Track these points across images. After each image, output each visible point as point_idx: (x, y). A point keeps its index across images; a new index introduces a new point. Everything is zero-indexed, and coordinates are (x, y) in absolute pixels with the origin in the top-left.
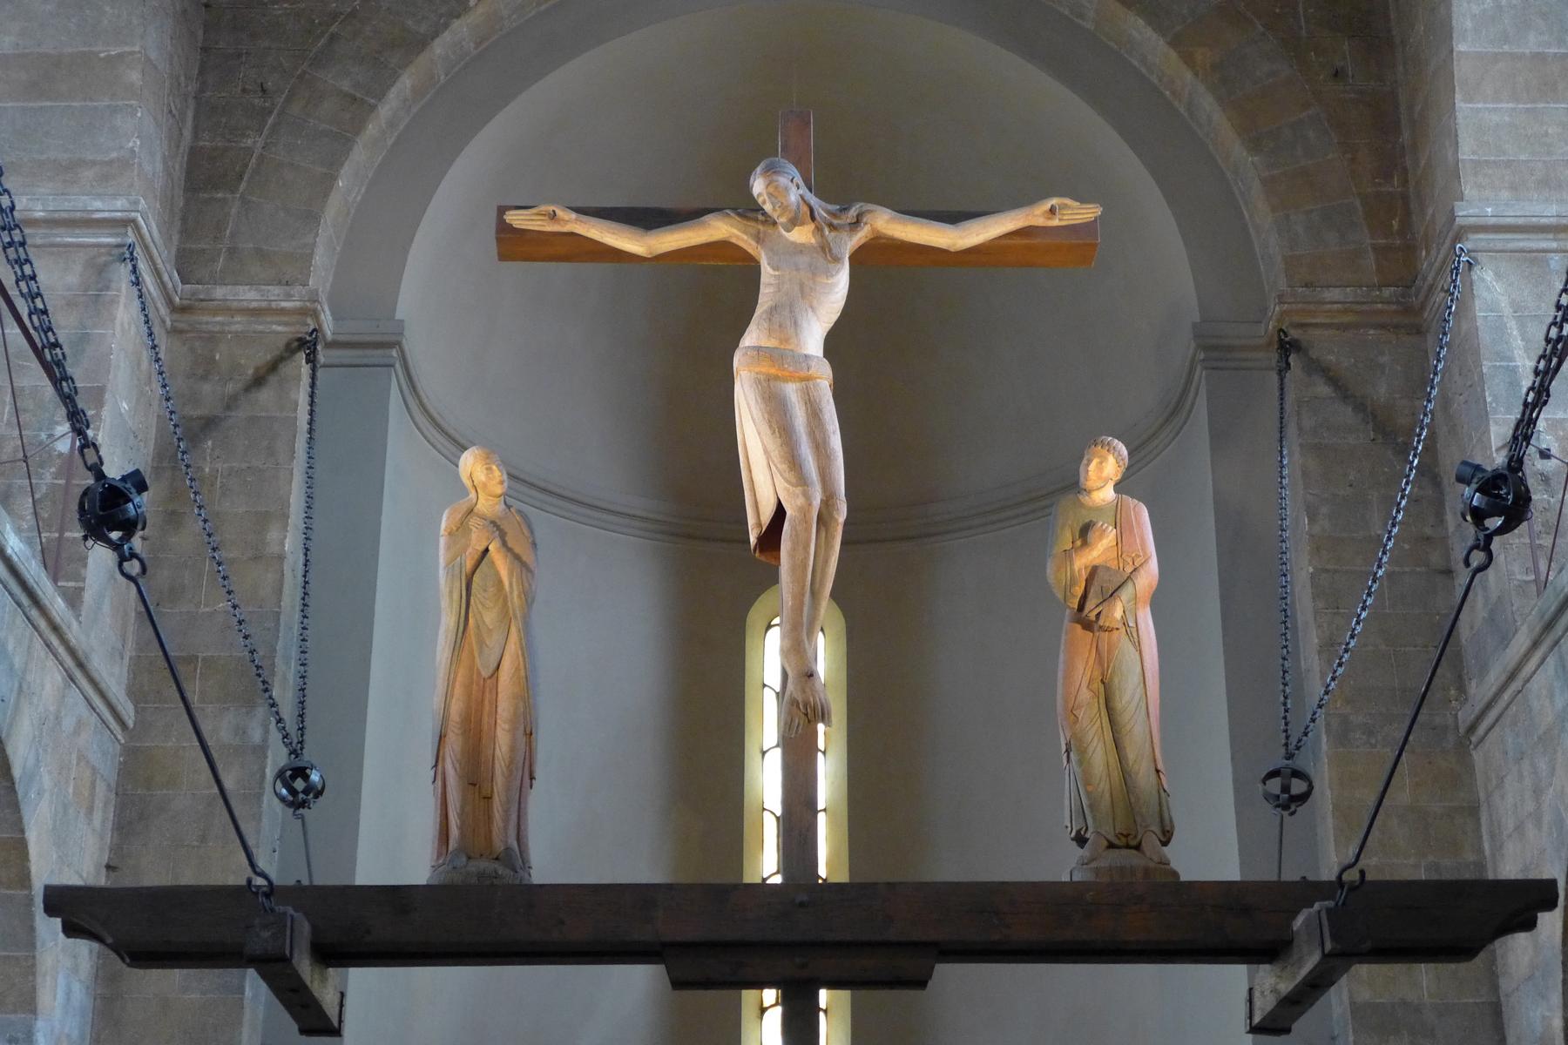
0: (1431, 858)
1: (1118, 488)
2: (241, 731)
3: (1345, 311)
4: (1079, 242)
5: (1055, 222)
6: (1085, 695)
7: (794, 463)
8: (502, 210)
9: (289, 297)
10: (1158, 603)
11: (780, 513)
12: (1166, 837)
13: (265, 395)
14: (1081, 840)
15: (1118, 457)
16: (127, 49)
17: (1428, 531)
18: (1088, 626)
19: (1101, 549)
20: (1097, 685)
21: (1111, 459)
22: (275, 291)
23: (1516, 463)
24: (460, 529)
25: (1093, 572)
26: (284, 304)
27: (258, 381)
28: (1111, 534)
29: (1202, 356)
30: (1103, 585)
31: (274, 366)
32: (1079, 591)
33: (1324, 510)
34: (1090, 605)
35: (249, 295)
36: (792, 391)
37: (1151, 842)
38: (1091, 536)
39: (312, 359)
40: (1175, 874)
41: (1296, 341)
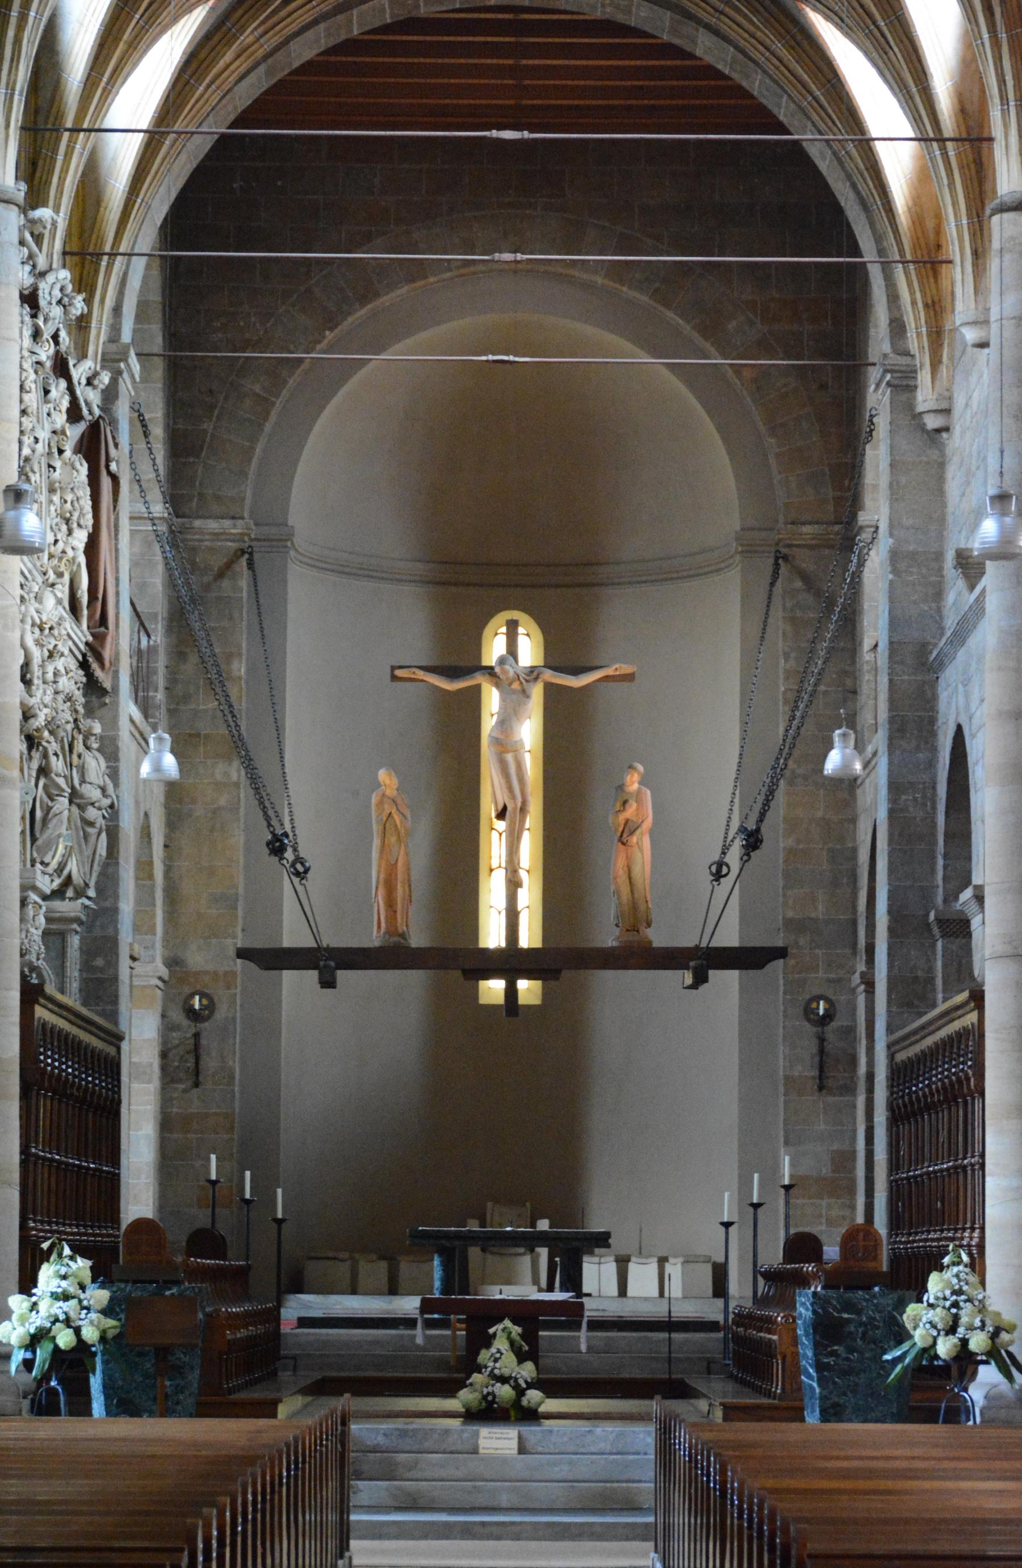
0: (831, 845)
1: (640, 783)
2: (226, 774)
3: (813, 539)
4: (629, 677)
5: (618, 673)
6: (621, 872)
7: (510, 789)
8: (393, 668)
9: (235, 526)
10: (652, 832)
11: (505, 808)
12: (649, 925)
13: (225, 583)
14: (617, 925)
15: (639, 773)
16: (153, 415)
17: (847, 668)
18: (623, 844)
19: (630, 812)
20: (626, 869)
21: (636, 775)
22: (227, 523)
23: (758, 830)
24: (380, 803)
25: (627, 821)
26: (233, 531)
27: (221, 575)
28: (634, 805)
29: (740, 549)
30: (630, 828)
31: (229, 565)
32: (621, 829)
33: (793, 655)
34: (625, 836)
35: (213, 525)
36: (509, 757)
37: (642, 928)
38: (627, 806)
39: (251, 565)
40: (650, 942)
41: (786, 555)
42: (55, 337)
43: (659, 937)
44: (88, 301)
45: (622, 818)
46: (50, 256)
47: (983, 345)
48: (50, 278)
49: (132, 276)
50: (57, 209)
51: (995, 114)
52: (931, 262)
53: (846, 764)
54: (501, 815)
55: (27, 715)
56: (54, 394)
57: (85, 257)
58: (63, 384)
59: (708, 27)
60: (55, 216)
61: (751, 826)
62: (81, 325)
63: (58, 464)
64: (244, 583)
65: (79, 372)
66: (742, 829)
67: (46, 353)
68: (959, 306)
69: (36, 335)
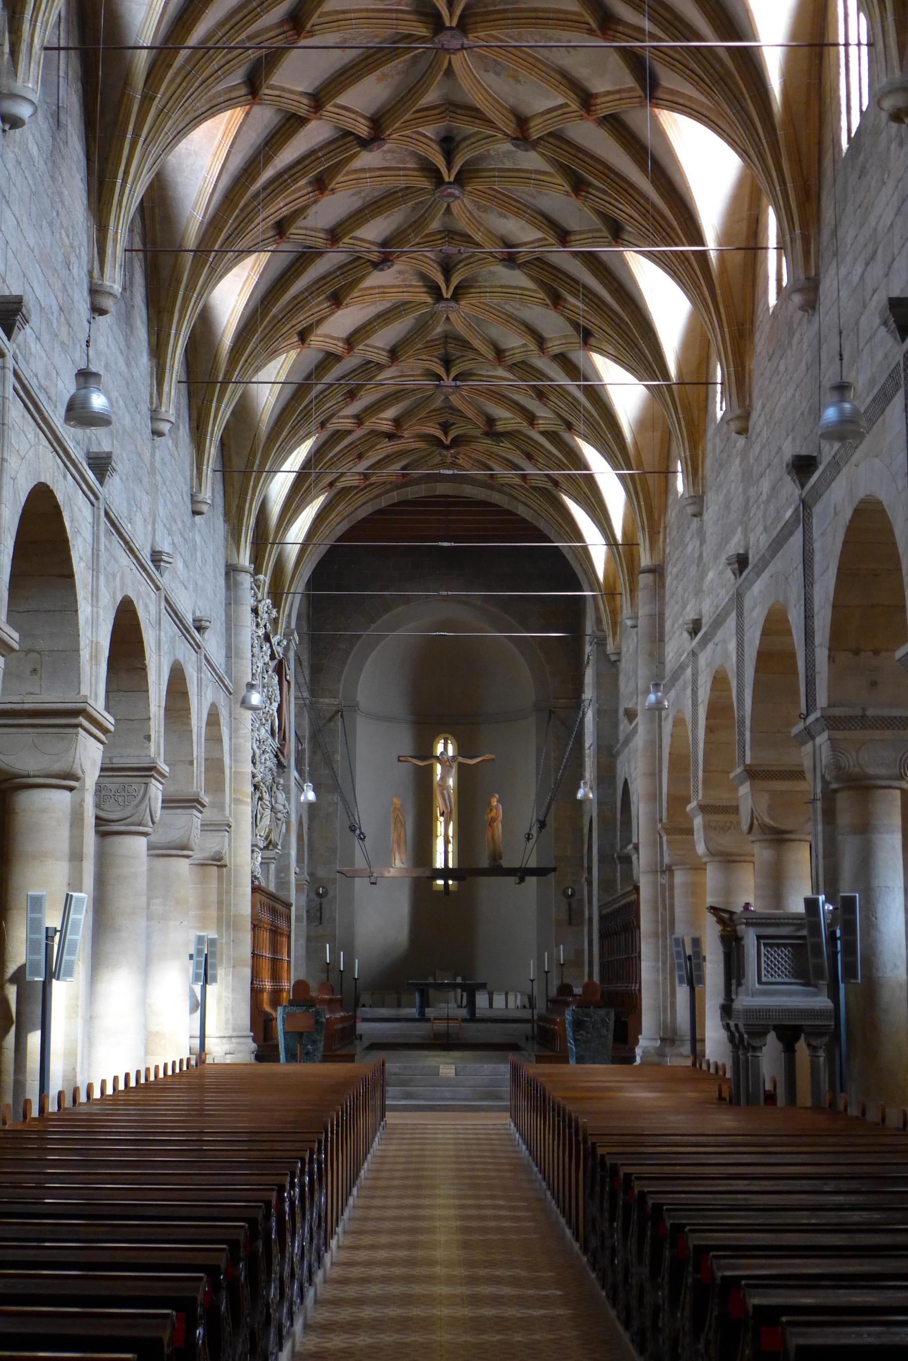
4: (492, 760)
7: (446, 805)
13: (332, 724)
19: (494, 813)
22: (332, 700)
30: (493, 820)
35: (327, 701)
36: (445, 792)
39: (342, 716)
42: (265, 626)
43: (506, 863)
44: (278, 612)
45: (490, 816)
46: (263, 594)
47: (635, 626)
48: (263, 603)
49: (294, 602)
50: (266, 576)
51: (640, 535)
52: (611, 593)
53: (586, 795)
54: (442, 815)
55: (254, 776)
56: (264, 648)
57: (277, 594)
58: (268, 645)
59: (522, 502)
60: (265, 578)
61: (542, 819)
62: (275, 621)
63: (266, 676)
64: (340, 723)
65: (275, 640)
66: (538, 820)
67: (261, 632)
68: (625, 612)
69: (258, 625)
